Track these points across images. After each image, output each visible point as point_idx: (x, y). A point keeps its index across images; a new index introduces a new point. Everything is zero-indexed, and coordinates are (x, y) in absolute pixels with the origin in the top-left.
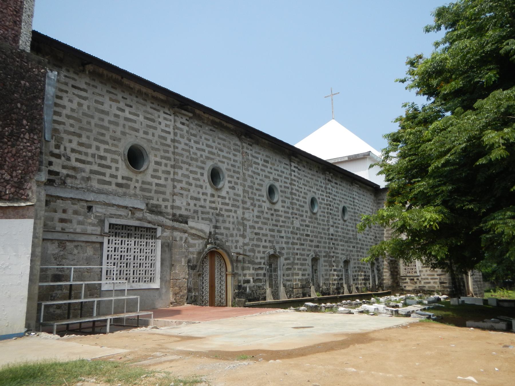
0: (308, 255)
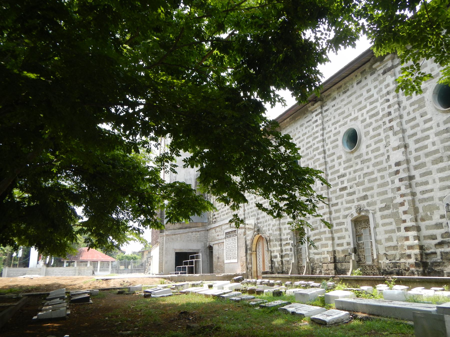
0: (346, 217)
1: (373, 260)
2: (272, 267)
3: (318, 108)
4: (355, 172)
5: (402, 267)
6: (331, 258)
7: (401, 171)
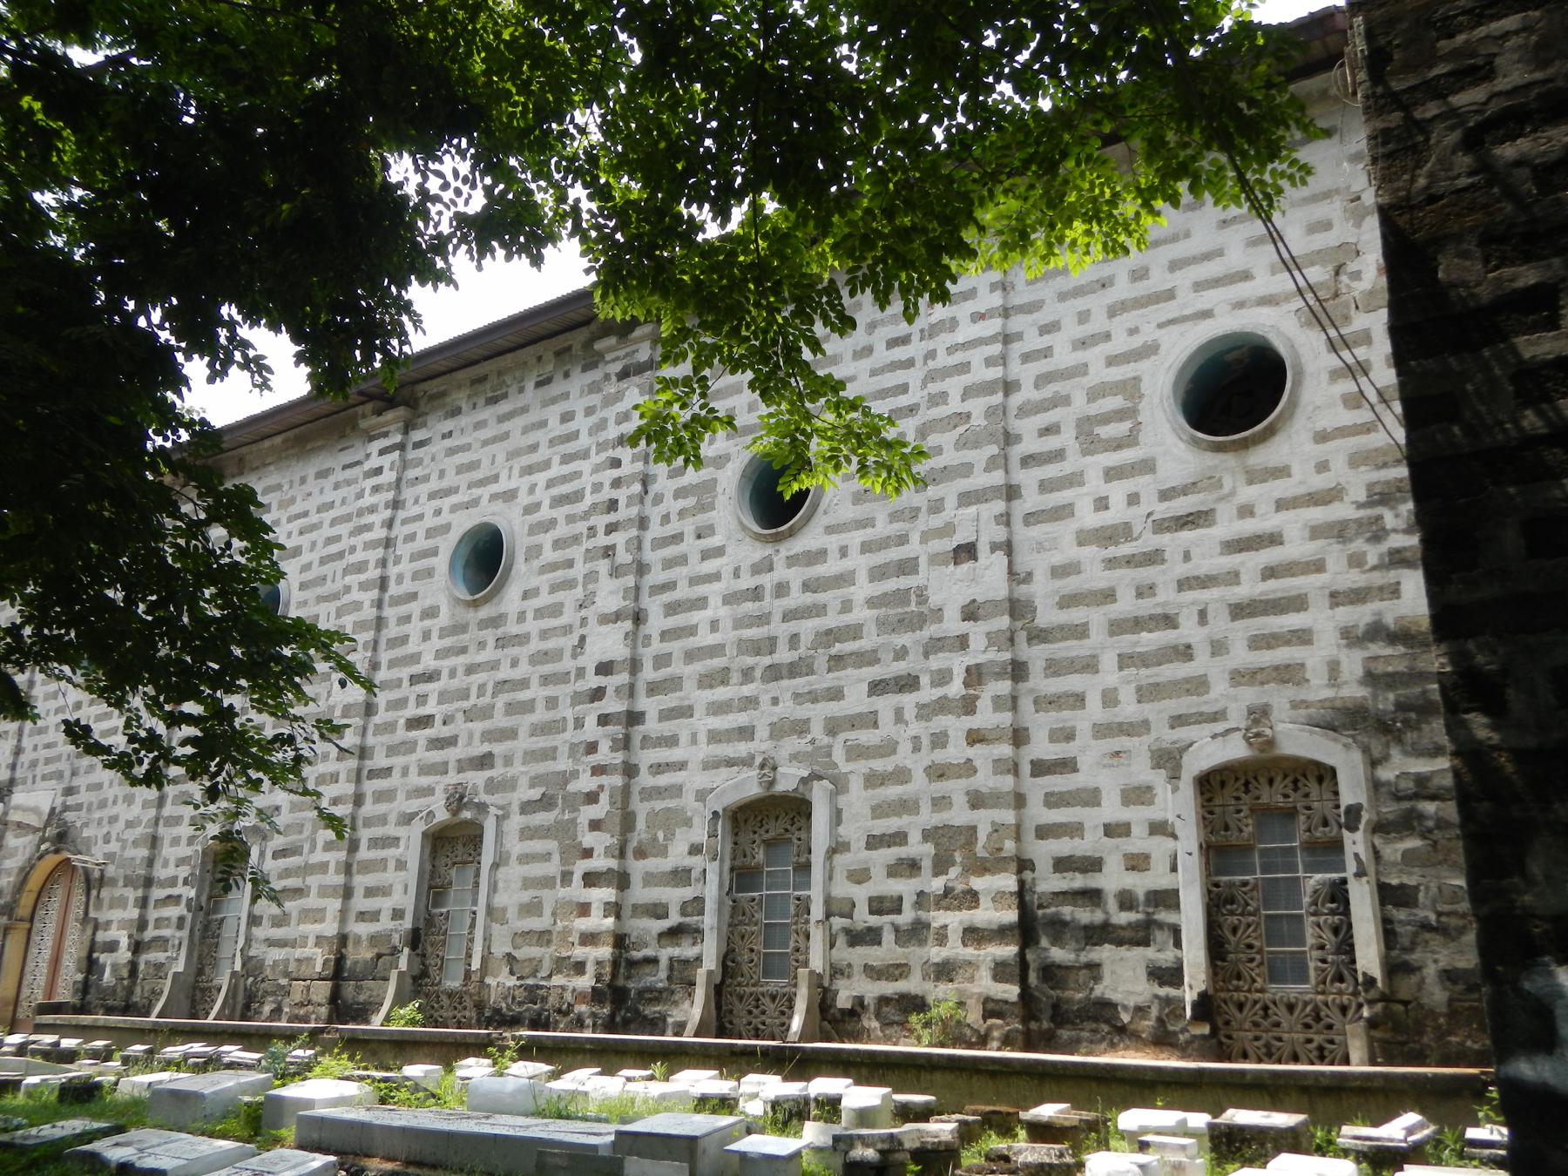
0: (407, 819)
1: (468, 975)
2: (85, 988)
3: (392, 428)
4: (471, 669)
5: (553, 1000)
6: (325, 962)
7: (610, 692)
